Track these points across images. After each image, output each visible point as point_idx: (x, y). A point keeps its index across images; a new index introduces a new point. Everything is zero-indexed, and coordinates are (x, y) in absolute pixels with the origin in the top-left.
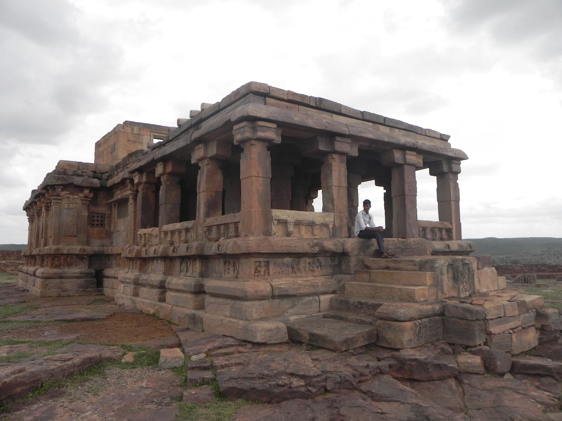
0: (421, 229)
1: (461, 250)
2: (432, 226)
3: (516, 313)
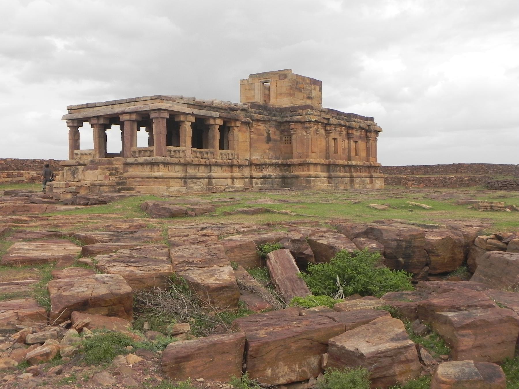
0: (132, 152)
1: (145, 162)
2: (139, 150)
3: (64, 186)
